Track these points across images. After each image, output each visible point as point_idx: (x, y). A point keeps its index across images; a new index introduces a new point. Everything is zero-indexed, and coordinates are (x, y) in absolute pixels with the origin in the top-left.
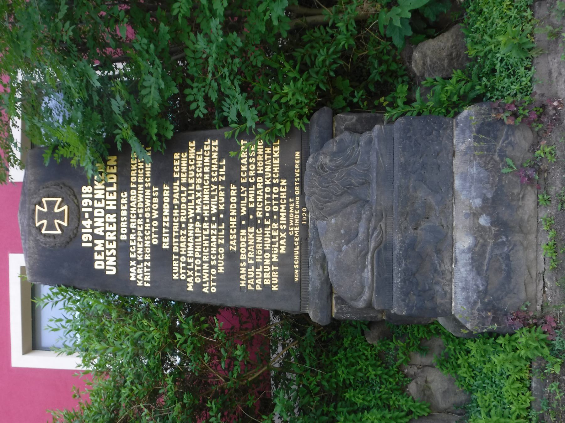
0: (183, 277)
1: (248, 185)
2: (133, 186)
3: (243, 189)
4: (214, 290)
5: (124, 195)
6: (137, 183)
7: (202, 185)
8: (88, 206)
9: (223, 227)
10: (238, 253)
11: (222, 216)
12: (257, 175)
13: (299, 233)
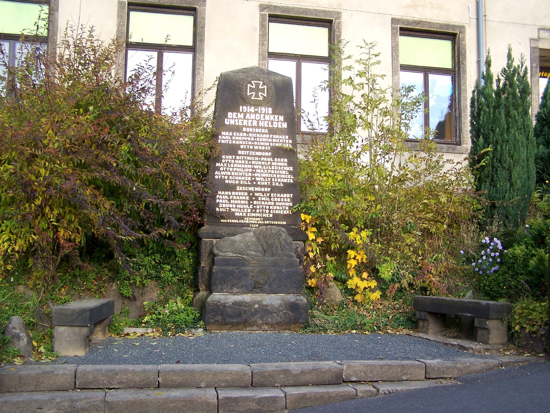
0: (223, 161)
1: (270, 197)
2: (271, 136)
3: (268, 195)
4: (216, 177)
6: (272, 138)
7: (271, 173)
8: (261, 111)
9: (249, 183)
10: (236, 191)
11: (255, 183)
12: (275, 202)
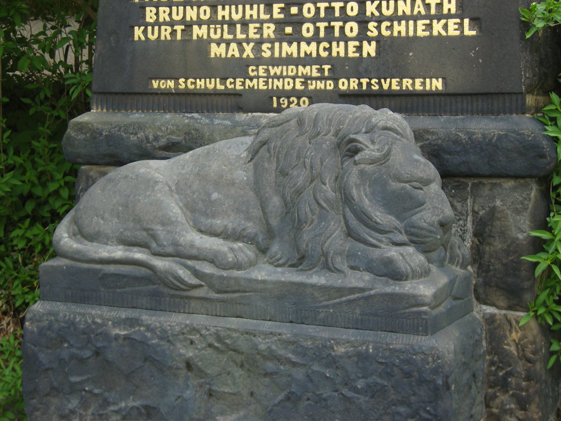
13: (252, 89)
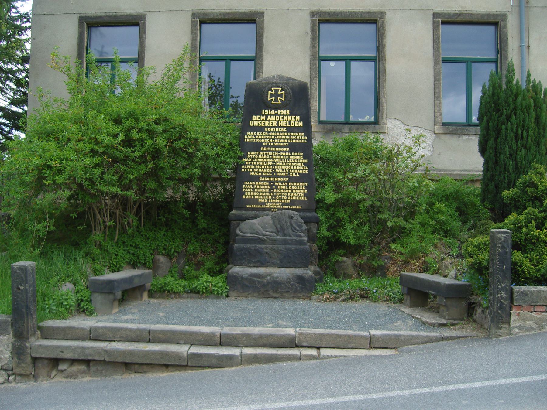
0: (249, 156)
1: (288, 186)
3: (286, 184)
4: (243, 170)
5: (285, 130)
6: (290, 136)
7: (288, 165)
12: (292, 190)
